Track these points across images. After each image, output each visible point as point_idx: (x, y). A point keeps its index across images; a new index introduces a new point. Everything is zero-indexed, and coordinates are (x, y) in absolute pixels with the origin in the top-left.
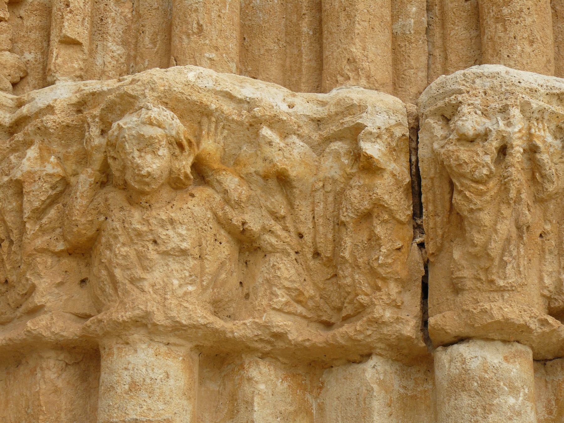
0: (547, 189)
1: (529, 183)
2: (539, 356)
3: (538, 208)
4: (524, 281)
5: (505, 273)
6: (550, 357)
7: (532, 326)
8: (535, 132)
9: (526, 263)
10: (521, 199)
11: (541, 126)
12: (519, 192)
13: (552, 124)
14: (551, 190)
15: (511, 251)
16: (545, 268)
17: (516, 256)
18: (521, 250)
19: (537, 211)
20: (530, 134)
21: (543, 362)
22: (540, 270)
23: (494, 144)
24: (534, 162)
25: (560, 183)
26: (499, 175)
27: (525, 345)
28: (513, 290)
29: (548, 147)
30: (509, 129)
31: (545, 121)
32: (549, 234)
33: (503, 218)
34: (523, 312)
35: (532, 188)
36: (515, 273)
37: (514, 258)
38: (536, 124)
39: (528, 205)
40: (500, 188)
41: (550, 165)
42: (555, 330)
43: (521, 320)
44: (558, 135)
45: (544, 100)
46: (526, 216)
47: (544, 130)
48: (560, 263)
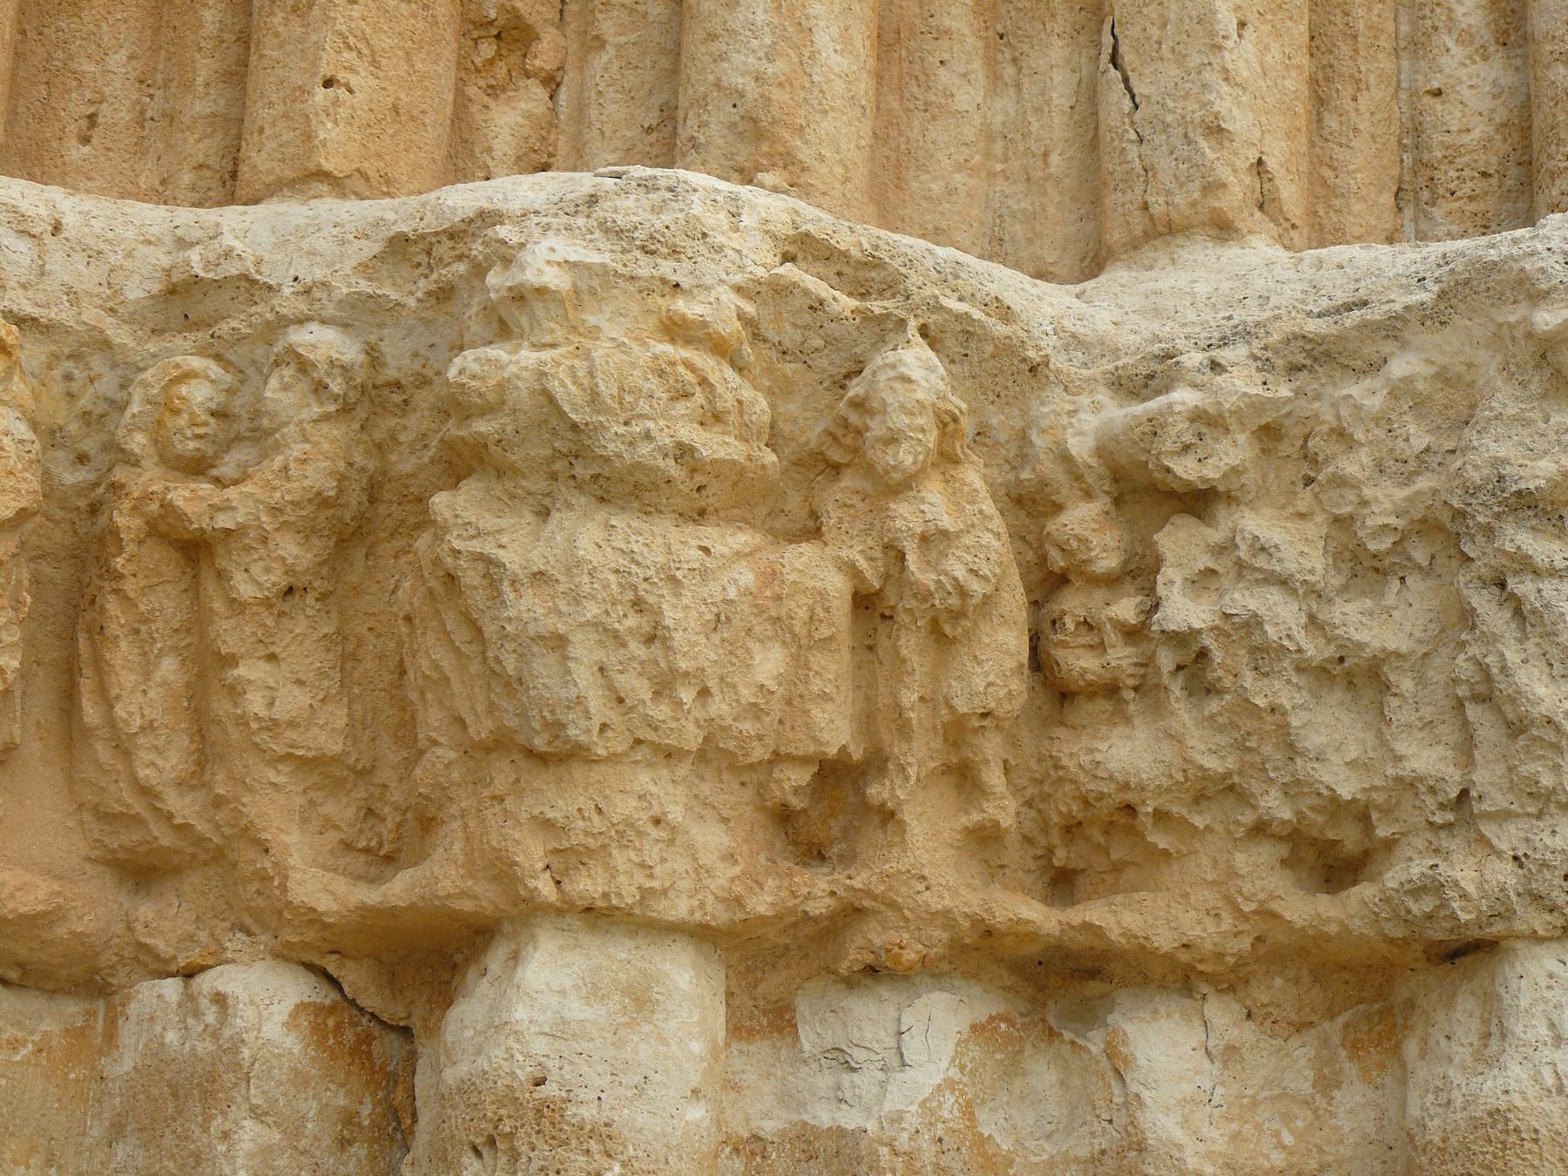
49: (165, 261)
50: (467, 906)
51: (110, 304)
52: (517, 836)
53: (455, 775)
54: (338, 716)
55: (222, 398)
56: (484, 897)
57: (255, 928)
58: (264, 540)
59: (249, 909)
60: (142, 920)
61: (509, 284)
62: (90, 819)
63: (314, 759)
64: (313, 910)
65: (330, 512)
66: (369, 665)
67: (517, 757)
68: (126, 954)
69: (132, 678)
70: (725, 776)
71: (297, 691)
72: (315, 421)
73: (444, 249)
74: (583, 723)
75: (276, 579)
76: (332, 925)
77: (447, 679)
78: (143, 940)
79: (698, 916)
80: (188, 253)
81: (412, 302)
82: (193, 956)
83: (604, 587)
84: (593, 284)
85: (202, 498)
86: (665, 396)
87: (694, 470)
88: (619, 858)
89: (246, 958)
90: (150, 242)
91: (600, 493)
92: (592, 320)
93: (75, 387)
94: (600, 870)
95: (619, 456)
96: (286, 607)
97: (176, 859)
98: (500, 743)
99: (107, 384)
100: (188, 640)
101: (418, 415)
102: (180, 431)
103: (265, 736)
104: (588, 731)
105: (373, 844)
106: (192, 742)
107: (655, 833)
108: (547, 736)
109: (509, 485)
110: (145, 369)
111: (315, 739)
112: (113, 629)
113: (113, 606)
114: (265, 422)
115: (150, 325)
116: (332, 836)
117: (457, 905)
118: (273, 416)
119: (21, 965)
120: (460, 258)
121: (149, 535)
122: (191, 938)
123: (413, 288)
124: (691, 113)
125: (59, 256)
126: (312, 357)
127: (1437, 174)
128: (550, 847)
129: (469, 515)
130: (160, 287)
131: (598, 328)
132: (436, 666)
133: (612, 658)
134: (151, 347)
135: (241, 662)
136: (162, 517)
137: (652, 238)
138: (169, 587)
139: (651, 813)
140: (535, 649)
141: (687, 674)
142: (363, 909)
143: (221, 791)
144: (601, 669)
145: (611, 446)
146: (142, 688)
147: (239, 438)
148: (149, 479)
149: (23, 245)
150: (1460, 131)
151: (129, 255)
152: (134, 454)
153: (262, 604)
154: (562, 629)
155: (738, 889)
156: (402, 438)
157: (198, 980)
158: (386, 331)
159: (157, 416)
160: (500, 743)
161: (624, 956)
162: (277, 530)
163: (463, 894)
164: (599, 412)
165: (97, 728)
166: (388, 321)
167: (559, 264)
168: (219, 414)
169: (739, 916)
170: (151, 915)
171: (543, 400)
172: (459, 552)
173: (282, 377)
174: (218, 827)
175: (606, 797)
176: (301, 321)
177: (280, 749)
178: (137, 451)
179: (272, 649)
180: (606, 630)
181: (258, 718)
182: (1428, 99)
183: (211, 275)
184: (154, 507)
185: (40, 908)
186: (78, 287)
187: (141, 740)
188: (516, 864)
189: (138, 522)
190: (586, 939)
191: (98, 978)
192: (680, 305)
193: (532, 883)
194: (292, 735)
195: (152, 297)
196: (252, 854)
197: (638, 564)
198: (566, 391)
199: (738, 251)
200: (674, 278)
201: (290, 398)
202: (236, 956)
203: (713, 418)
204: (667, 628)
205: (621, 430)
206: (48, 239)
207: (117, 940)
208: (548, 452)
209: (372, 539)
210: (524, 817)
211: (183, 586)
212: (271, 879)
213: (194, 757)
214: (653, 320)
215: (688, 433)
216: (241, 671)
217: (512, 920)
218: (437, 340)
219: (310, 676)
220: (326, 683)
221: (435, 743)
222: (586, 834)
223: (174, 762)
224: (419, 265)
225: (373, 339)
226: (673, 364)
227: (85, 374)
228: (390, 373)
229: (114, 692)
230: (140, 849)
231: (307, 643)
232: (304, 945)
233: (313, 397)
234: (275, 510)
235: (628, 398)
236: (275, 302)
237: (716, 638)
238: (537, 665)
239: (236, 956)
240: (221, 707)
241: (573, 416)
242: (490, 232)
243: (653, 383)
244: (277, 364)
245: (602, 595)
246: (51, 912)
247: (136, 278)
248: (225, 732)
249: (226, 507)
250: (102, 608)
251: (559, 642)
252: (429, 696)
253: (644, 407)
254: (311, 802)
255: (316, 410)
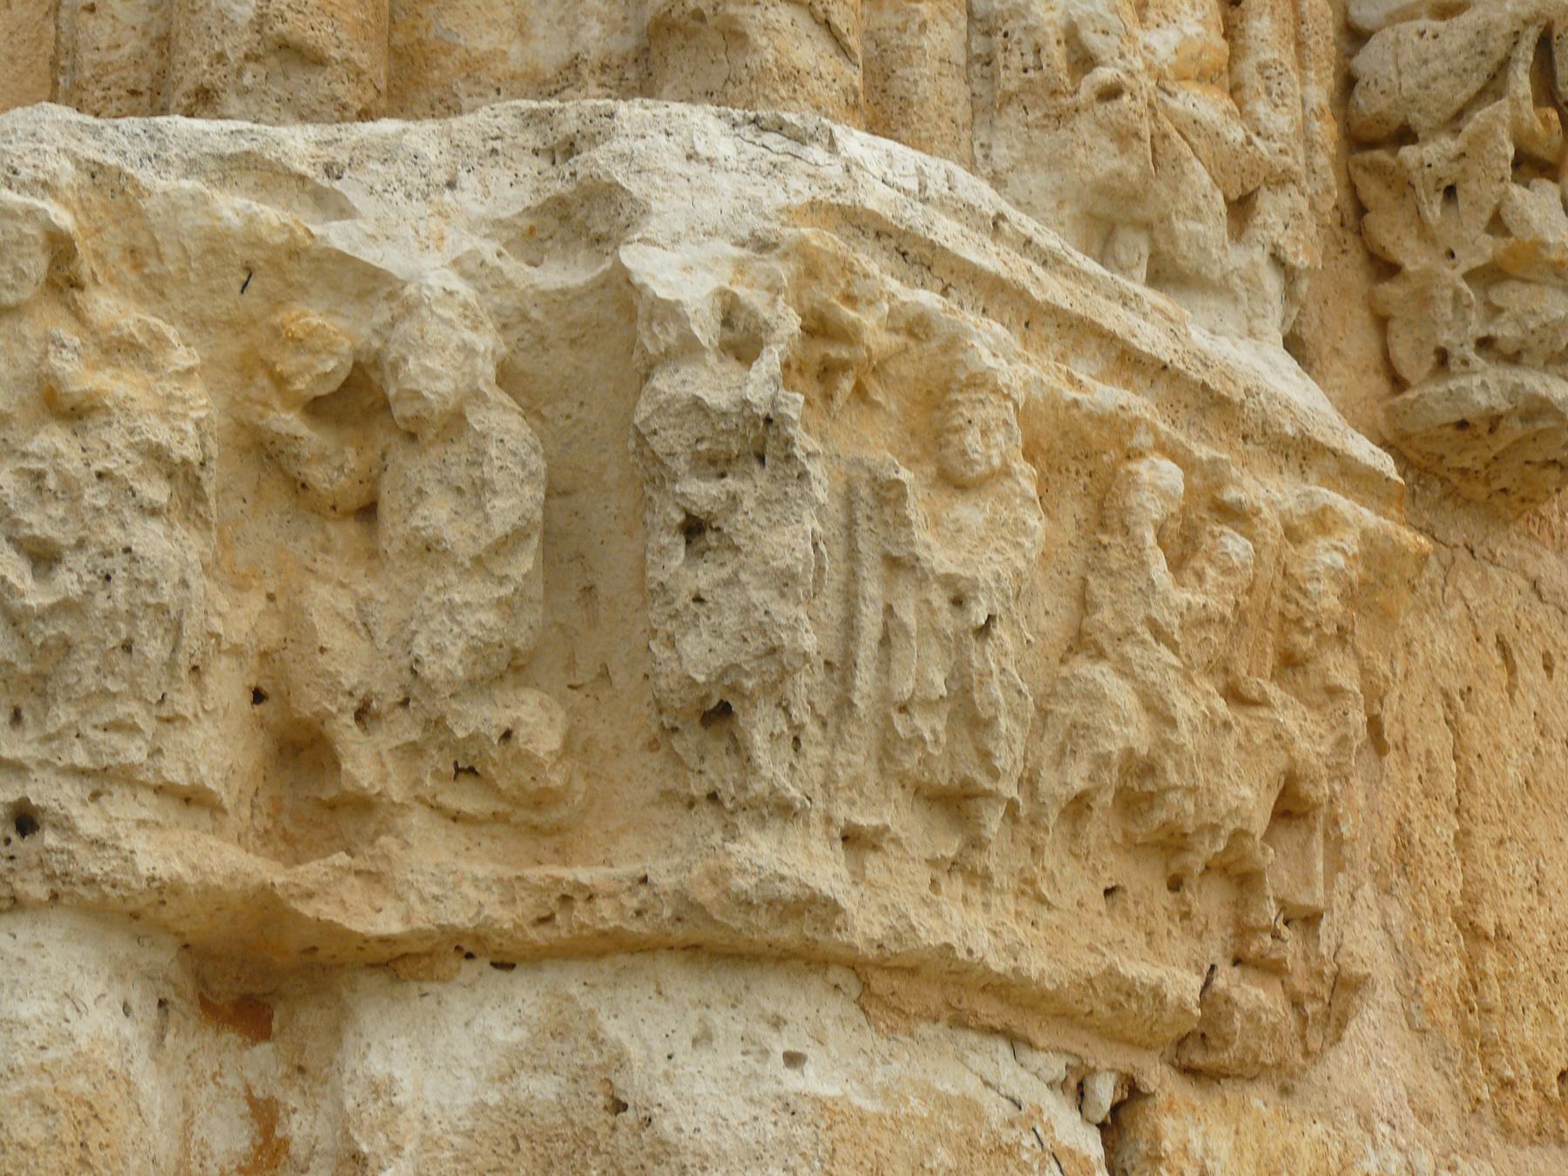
127: (85, 95)
150: (109, 48)
182: (85, 16)
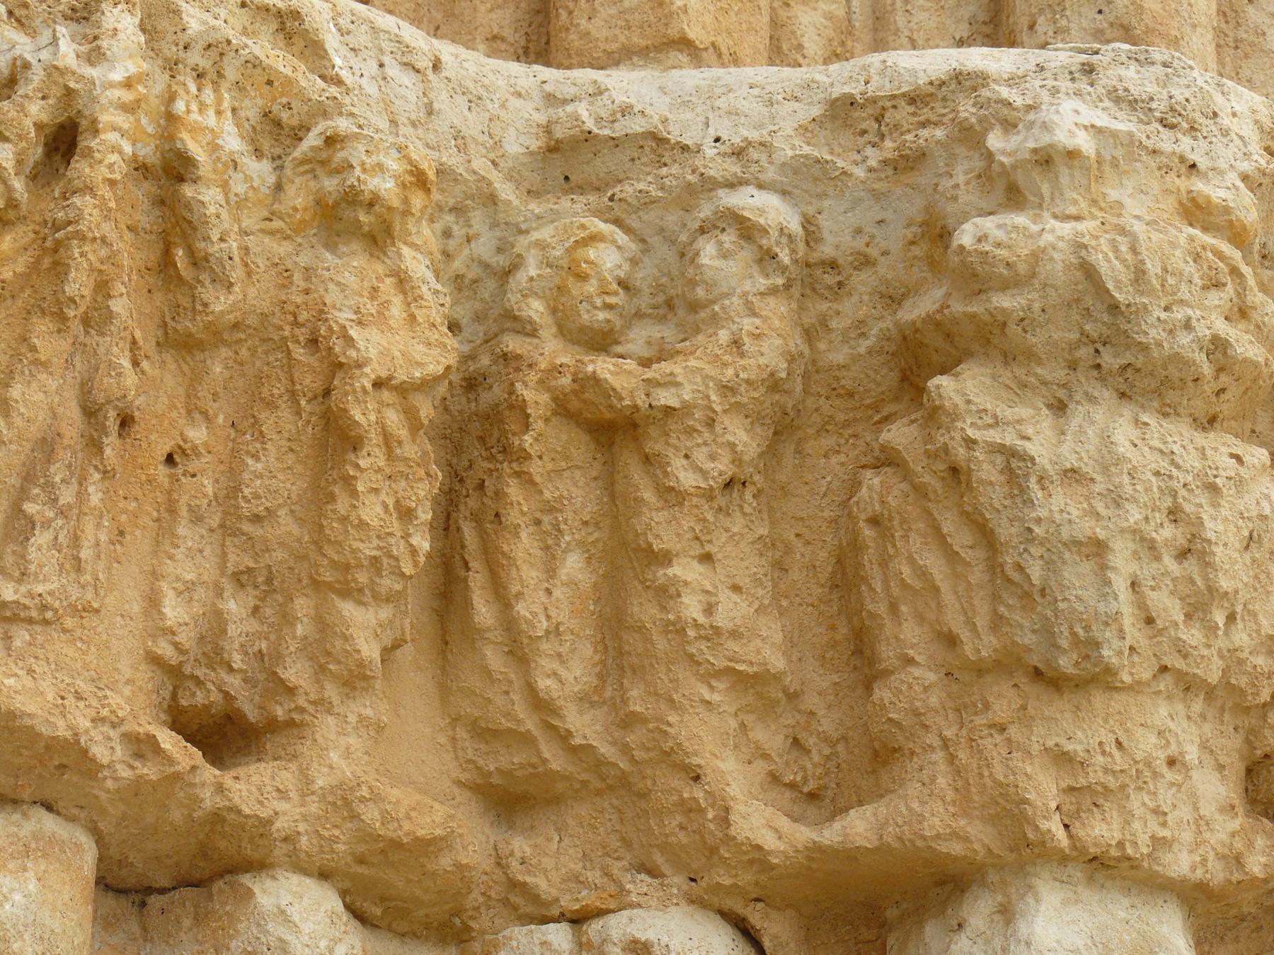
0: (206, 305)
1: (152, 280)
2: (124, 872)
3: (172, 366)
4: (89, 595)
5: (23, 557)
6: (164, 882)
7: (100, 752)
8: (188, 111)
9: (103, 537)
10: (110, 316)
11: (208, 95)
12: (103, 288)
13: (247, 103)
14: (218, 308)
15: (53, 485)
16: (169, 567)
17: (70, 507)
18: (91, 489)
19: (166, 376)
20: (171, 117)
21: (137, 898)
22: (154, 573)
23: (35, 111)
24: (173, 210)
25: (252, 292)
26: (37, 218)
27: (72, 819)
28: (46, 622)
29: (225, 164)
30: (89, 71)
31: (225, 85)
32: (198, 455)
33: (37, 362)
34: (70, 700)
35: (159, 297)
36: (61, 566)
37: (62, 513)
38: (193, 88)
39: (134, 342)
40: (38, 261)
41: (226, 225)
42: (177, 776)
43: (61, 723)
44: (266, 145)
45: (231, 20)
46: (119, 375)
47: (219, 113)
48: (224, 555)
49: (541, 118)
50: (956, 848)
51: (492, 156)
52: (1029, 769)
53: (934, 700)
54: (772, 629)
55: (626, 267)
56: (979, 837)
57: (666, 869)
58: (711, 423)
59: (665, 848)
60: (518, 854)
61: (1031, 145)
62: (465, 735)
63: (756, 676)
64: (759, 848)
65: (777, 397)
66: (796, 575)
67: (1023, 680)
68: (493, 894)
69: (534, 574)
70: (1227, 717)
71: (735, 597)
72: (761, 294)
73: (903, 114)
74: (1116, 643)
75: (722, 467)
76: (773, 867)
77: (936, 590)
78: (520, 878)
79: (1199, 873)
80: (569, 108)
81: (859, 172)
82: (587, 898)
83: (1146, 490)
84: (1122, 154)
85: (630, 372)
86: (1200, 283)
87: (1220, 370)
88: (1137, 802)
89: (654, 903)
90: (520, 95)
91: (1123, 387)
92: (1113, 194)
93: (452, 245)
94: (1115, 814)
95: (1159, 345)
96: (722, 501)
97: (560, 786)
98: (1008, 663)
99: (484, 247)
100: (596, 535)
101: (855, 299)
102: (589, 299)
103: (703, 645)
104: (1120, 653)
105: (798, 779)
106: (596, 652)
107: (1170, 775)
108: (1075, 657)
109: (1020, 372)
110: (527, 232)
111: (758, 652)
112: (512, 516)
113: (514, 490)
114: (700, 292)
115: (526, 185)
116: (761, 766)
117: (943, 847)
118: (710, 286)
119: (383, 899)
120: (923, 125)
121: (555, 413)
122: (576, 879)
123: (858, 158)
124: (1041, 20)
125: (444, 96)
126: (762, 221)
128: (1064, 785)
129: (983, 401)
130: (539, 143)
131: (1120, 204)
132: (923, 574)
133: (1147, 571)
134: (535, 207)
135: (675, 561)
136: (575, 392)
137: (1172, 109)
138: (578, 473)
139: (1169, 752)
140: (1067, 555)
141: (1226, 593)
142: (816, 850)
143: (638, 709)
144: (1133, 584)
145: (1153, 333)
146: (549, 586)
147: (639, 315)
148: (551, 350)
149: (407, 79)
151: (503, 106)
152: (531, 322)
153: (703, 496)
154: (1101, 534)
155: (1239, 845)
156: (833, 324)
157: (593, 929)
158: (826, 203)
159: (557, 281)
160: (1008, 663)
161: (1123, 914)
162: (725, 411)
163: (955, 835)
164: (1142, 293)
165: (489, 629)
166: (831, 191)
167: (1086, 127)
168: (624, 284)
169: (1237, 877)
170: (528, 851)
171: (1079, 275)
172: (974, 442)
173: (720, 243)
174: (625, 749)
175: (1127, 731)
176: (733, 184)
177: (720, 663)
178: (536, 317)
179: (708, 548)
180: (1143, 539)
181: (697, 625)
183: (606, 132)
184: (565, 381)
185: (438, 832)
186: (466, 132)
187: (544, 646)
188: (1026, 801)
189: (544, 398)
190: (1085, 893)
191: (457, 921)
192: (1199, 186)
193: (1044, 825)
194: (733, 646)
195: (531, 154)
196: (676, 782)
197: (1178, 467)
198: (1112, 270)
199: (1242, 138)
200: (1193, 157)
201: (732, 267)
202: (642, 900)
203: (1242, 312)
204: (1209, 541)
205: (1163, 315)
206: (431, 75)
207: (485, 878)
208: (1074, 336)
209: (800, 434)
210: (1035, 748)
211: (594, 474)
212: (702, 811)
213: (598, 669)
214: (1170, 203)
215: (1222, 327)
216: (676, 570)
217: (1001, 867)
218: (889, 215)
219: (744, 582)
220: (760, 592)
221: (910, 661)
222: (1106, 771)
223: (578, 673)
224: (864, 132)
225: (811, 210)
226: (1204, 248)
227: (463, 231)
228: (826, 251)
229: (514, 589)
230: (519, 773)
231: (742, 545)
232: (734, 890)
233: (756, 268)
234: (727, 389)
235: (1171, 281)
236: (698, 162)
237: (1247, 556)
238: (1068, 574)
239: (642, 900)
240: (645, 611)
241: (1117, 295)
242: (985, 93)
243: (1190, 268)
244: (702, 231)
245: (1143, 498)
246: (442, 839)
247: (512, 131)
248: (648, 640)
249: (671, 382)
250: (499, 495)
251: (1097, 549)
252: (904, 608)
253: (1184, 292)
254: (743, 725)
255: (762, 283)
